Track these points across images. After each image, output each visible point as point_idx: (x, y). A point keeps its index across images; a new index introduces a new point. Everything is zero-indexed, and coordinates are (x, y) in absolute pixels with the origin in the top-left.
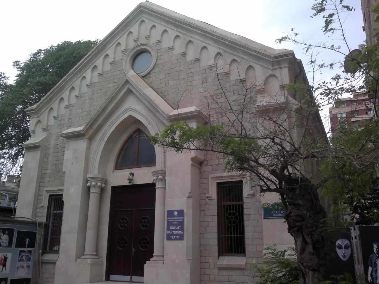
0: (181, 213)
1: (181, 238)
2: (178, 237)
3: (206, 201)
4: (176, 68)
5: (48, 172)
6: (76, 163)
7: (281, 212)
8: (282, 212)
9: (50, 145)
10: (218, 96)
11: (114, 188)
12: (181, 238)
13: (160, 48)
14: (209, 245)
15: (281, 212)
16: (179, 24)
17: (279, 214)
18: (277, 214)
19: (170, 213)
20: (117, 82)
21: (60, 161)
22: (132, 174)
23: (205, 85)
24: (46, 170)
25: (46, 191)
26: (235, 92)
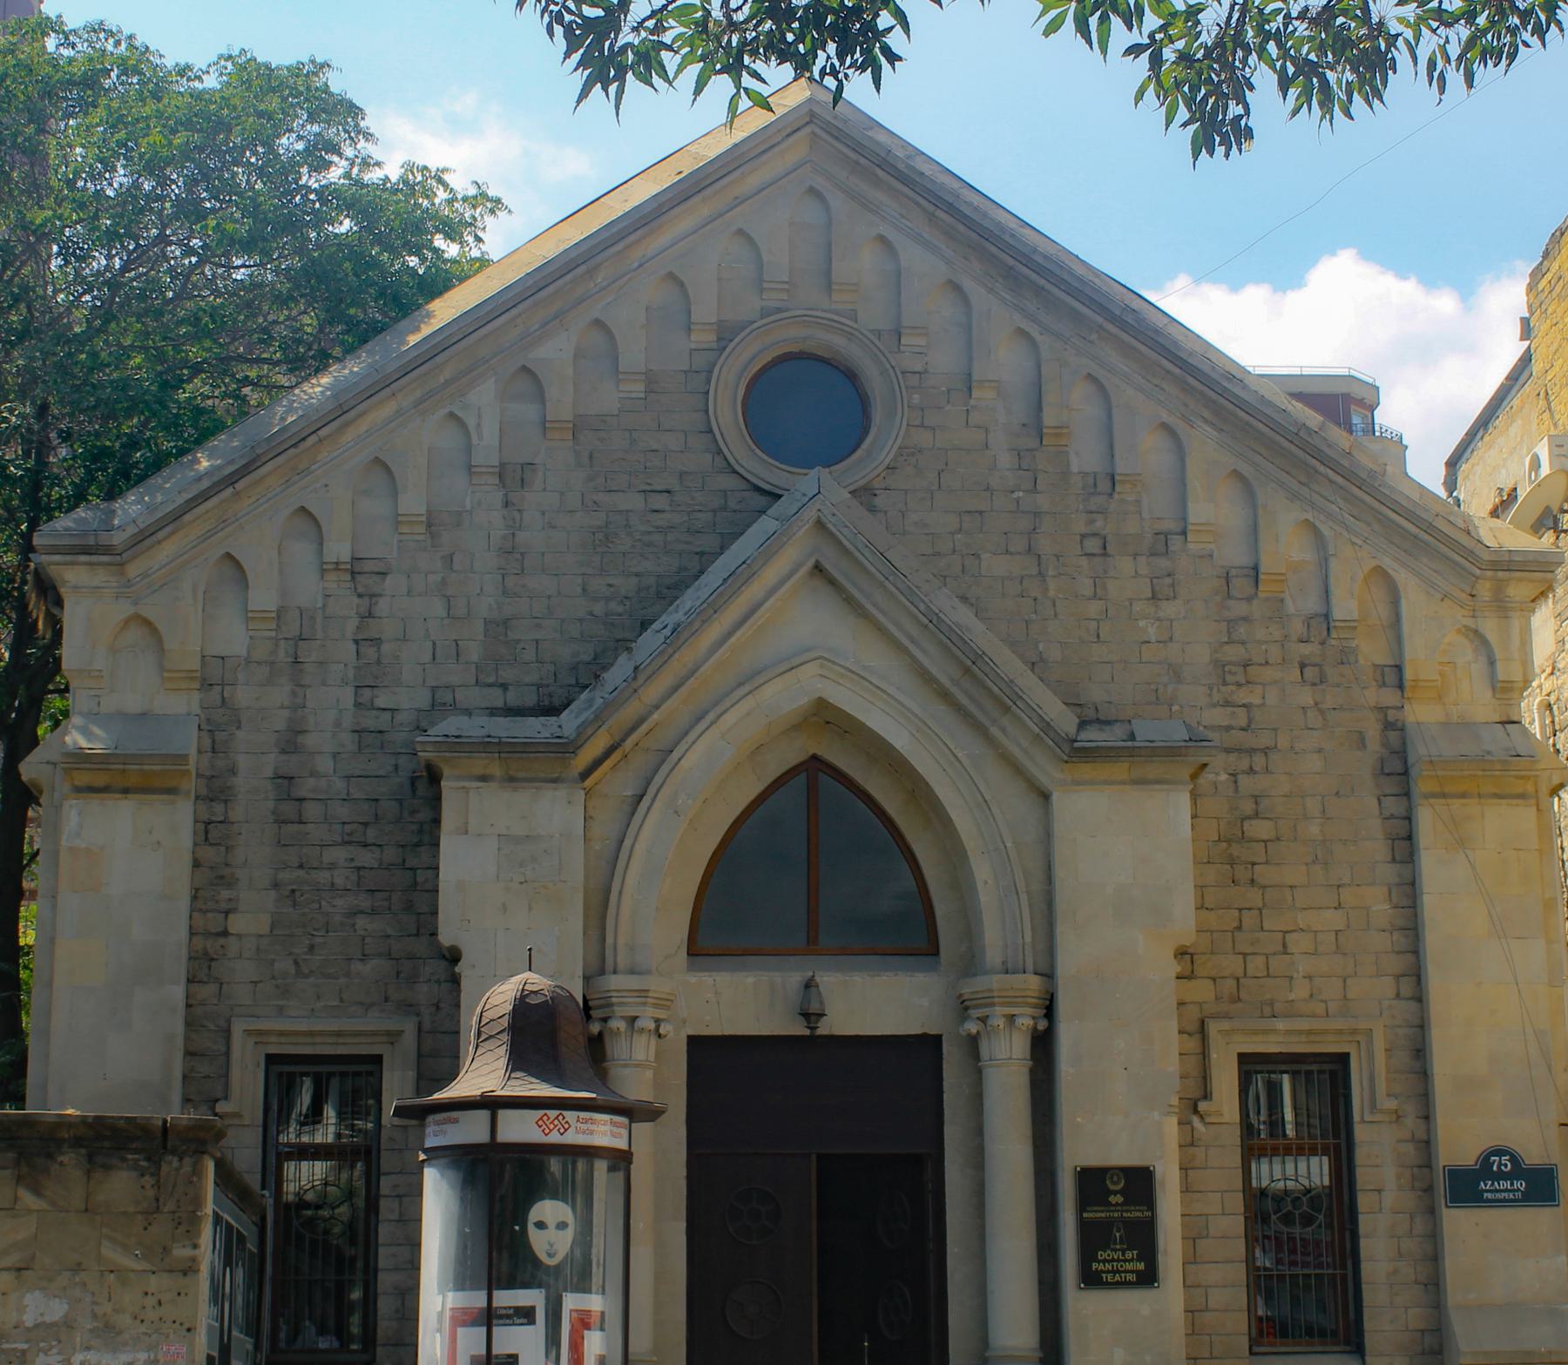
0: (1140, 1182)
1: (1148, 1278)
2: (1131, 1277)
3: (1193, 1129)
4: (1013, 492)
5: (237, 924)
6: (530, 909)
7: (1512, 1184)
8: (1517, 1184)
9: (233, 771)
10: (1230, 672)
11: (693, 1041)
12: (1148, 1278)
13: (918, 368)
14: (1207, 1309)
15: (1512, 1184)
16: (1042, 282)
17: (1506, 1190)
18: (1497, 1191)
19: (1092, 1181)
20: (669, 492)
21: (327, 874)
22: (809, 985)
23: (1170, 609)
24: (227, 913)
25: (248, 1032)
26: (1308, 672)
